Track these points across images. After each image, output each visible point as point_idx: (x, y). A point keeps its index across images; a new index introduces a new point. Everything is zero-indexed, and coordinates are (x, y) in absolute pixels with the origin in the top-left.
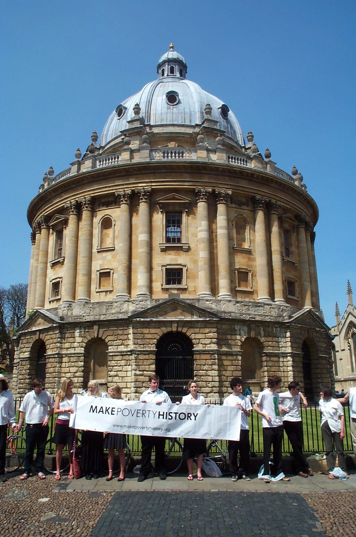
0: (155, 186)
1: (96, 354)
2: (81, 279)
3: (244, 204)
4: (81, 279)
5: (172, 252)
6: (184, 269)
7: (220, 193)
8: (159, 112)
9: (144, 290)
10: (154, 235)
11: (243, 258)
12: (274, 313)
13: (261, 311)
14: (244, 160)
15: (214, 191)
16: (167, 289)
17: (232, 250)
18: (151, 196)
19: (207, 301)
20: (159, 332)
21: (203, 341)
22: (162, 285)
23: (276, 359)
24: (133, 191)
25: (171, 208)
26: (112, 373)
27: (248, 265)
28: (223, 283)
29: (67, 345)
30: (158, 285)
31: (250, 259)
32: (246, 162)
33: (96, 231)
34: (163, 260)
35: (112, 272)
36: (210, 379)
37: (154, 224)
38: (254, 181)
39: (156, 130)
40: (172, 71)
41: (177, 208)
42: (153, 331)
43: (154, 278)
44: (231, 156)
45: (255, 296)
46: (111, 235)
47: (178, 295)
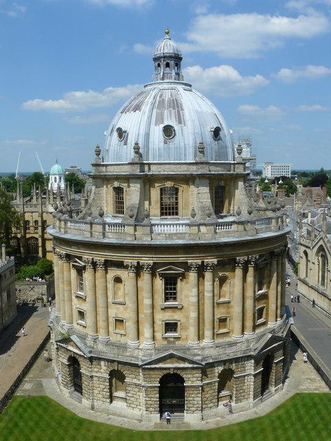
0: (156, 260)
1: (117, 376)
2: (101, 324)
4: (101, 324)
5: (170, 311)
6: (179, 323)
8: (156, 146)
9: (150, 342)
10: (156, 296)
11: (224, 308)
12: (244, 347)
13: (234, 349)
18: (153, 270)
19: (195, 349)
20: (160, 375)
24: (138, 263)
26: (129, 395)
28: (208, 333)
29: (96, 370)
33: (110, 285)
34: (162, 317)
35: (125, 321)
36: (196, 402)
37: (155, 288)
40: (168, 65)
41: (174, 276)
42: (157, 373)
43: (156, 329)
46: (122, 289)
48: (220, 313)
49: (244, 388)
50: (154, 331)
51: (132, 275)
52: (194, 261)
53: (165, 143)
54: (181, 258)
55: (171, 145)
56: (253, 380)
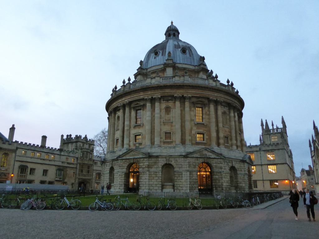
0: (130, 100)
3: (170, 100)
6: (141, 135)
7: (155, 98)
10: (132, 121)
14: (171, 78)
15: (152, 97)
16: (135, 144)
17: (162, 123)
21: (143, 167)
22: (133, 143)
23: (181, 173)
24: (123, 104)
25: (137, 108)
27: (171, 129)
30: (131, 144)
31: (172, 126)
32: (172, 79)
36: (144, 183)
38: (173, 88)
39: (149, 70)
41: (139, 108)
43: (131, 140)
44: (164, 78)
45: (174, 143)
47: (139, 146)
48: (166, 128)
49: (182, 181)
50: (130, 141)
51: (121, 111)
52: (148, 95)
53: (155, 58)
54: (141, 95)
55: (157, 58)
56: (188, 175)
